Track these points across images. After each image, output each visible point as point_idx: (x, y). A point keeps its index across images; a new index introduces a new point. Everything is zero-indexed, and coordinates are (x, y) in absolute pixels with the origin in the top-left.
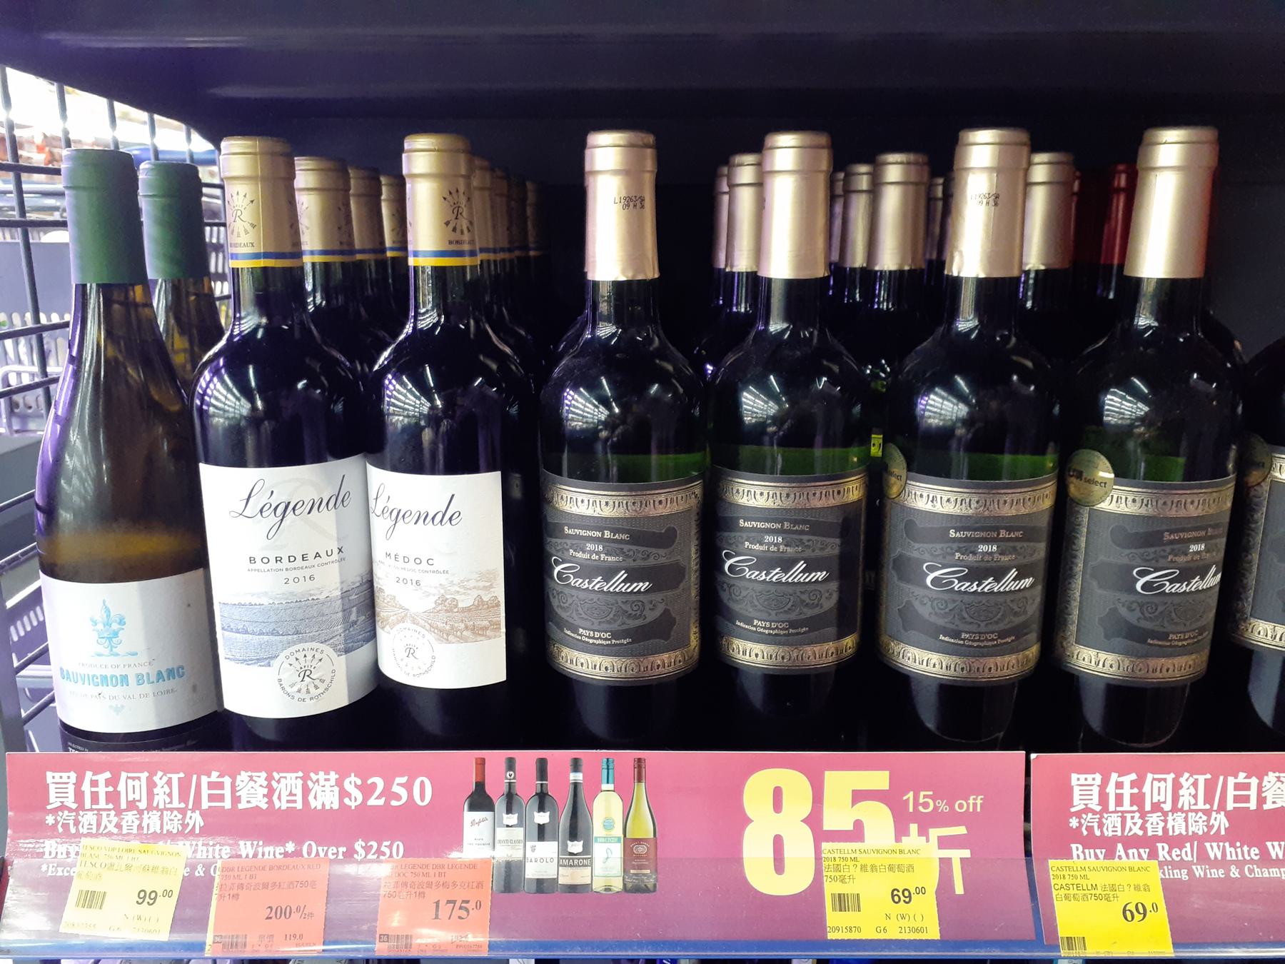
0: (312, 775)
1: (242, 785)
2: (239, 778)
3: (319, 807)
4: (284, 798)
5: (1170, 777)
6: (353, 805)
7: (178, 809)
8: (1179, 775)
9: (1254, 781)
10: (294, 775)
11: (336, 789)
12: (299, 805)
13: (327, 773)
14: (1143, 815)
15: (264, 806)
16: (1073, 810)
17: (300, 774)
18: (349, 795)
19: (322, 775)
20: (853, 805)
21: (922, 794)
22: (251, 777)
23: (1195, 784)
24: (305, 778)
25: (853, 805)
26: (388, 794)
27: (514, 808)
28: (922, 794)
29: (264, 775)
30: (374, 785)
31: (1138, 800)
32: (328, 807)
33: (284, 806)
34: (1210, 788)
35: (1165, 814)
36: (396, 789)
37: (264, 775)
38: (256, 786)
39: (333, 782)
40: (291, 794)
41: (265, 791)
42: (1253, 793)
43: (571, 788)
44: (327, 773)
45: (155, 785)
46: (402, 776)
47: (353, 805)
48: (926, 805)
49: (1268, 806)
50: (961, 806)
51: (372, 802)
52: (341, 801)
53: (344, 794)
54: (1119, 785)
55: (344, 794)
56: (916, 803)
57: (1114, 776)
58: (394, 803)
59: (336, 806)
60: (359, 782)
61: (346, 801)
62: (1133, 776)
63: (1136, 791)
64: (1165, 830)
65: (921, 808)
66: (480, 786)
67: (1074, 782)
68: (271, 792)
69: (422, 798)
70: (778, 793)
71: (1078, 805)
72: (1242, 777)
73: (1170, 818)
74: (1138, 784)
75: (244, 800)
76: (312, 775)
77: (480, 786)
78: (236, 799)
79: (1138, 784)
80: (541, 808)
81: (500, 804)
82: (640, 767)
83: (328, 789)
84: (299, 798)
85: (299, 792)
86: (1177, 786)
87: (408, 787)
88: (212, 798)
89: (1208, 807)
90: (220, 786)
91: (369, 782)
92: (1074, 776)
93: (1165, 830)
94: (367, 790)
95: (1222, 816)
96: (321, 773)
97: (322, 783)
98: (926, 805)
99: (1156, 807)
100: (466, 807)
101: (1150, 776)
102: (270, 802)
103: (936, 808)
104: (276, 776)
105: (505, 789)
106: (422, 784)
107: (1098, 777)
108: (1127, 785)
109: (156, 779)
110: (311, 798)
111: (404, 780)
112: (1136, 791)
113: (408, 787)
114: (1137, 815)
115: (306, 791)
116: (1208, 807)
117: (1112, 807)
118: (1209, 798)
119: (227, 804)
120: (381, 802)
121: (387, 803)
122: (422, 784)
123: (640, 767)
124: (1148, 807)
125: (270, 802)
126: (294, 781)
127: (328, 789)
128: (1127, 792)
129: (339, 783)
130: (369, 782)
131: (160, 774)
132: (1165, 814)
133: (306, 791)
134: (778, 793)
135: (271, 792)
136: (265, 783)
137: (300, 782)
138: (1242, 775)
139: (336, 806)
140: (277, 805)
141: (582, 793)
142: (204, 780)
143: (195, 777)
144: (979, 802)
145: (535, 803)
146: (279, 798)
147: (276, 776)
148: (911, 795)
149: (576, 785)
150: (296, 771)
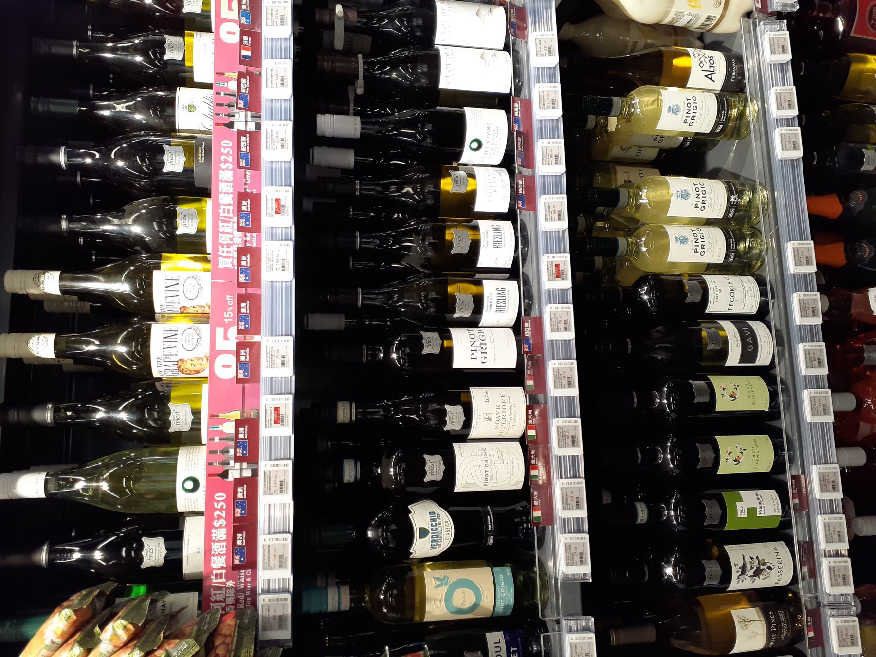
0: (213, 539)
1: (216, 566)
2: (214, 567)
3: (226, 536)
4: (222, 549)
5: (220, 234)
6: (225, 523)
7: (226, 591)
8: (219, 232)
9: (222, 207)
10: (213, 546)
11: (219, 529)
12: (225, 544)
13: (212, 533)
14: (233, 244)
15: (225, 557)
16: (232, 268)
17: (212, 544)
18: (221, 525)
19: (213, 535)
20: (229, 340)
21: (225, 316)
22: (214, 562)
23: (223, 226)
24: (214, 541)
25: (229, 340)
26: (221, 509)
27: (227, 462)
28: (225, 316)
29: (212, 558)
30: (218, 515)
31: (228, 246)
32: (226, 533)
33: (225, 549)
34: (224, 222)
35: (234, 237)
36: (219, 507)
37: (212, 558)
38: (217, 560)
39: (216, 531)
40: (220, 547)
41: (219, 557)
42: (227, 208)
43: (221, 441)
44: (212, 533)
45: (216, 600)
46: (214, 505)
47: (225, 523)
48: (230, 315)
49: (232, 203)
50: (230, 303)
51: (224, 516)
52: (223, 527)
53: (221, 526)
54: (223, 252)
55: (221, 526)
56: (229, 318)
57: (220, 253)
58: (225, 507)
59: (225, 529)
60: (216, 521)
61: (223, 525)
62: (220, 247)
63: (225, 246)
64: (240, 237)
65: (231, 316)
66: (219, 475)
67: (222, 267)
68: (219, 555)
69: (223, 496)
70: (224, 366)
71: (230, 266)
72: (221, 211)
73: (235, 235)
74: (223, 245)
75: (222, 565)
76: (213, 539)
77: (219, 475)
78: (222, 568)
79: (223, 245)
80: (228, 452)
81: (226, 468)
82: (213, 416)
83: (218, 533)
84: (222, 544)
85: (219, 544)
86: (223, 233)
87: (218, 502)
88: (221, 577)
89: (231, 223)
90: (216, 575)
91: (216, 517)
92: (219, 266)
93: (240, 237)
94: (219, 517)
95: (234, 218)
96: (212, 535)
97: (216, 535)
98: (230, 315)
99: (231, 240)
100: (227, 480)
101: (220, 241)
102: (224, 555)
103: (231, 311)
104: (212, 553)
105: (221, 466)
106: (218, 497)
107: (220, 259)
108: (223, 249)
109: (213, 600)
110: (222, 539)
111: (216, 504)
112: (225, 246)
113: (218, 502)
114: (234, 246)
115: (219, 541)
116: (231, 223)
117: (231, 255)
118: (228, 222)
119: (224, 571)
120: (224, 512)
121: (224, 510)
122: (218, 497)
123: (213, 416)
124: (231, 242)
125: (224, 555)
126: (215, 546)
127: (218, 533)
128: (225, 249)
129: (216, 528)
130: (216, 517)
131: (211, 598)
132: (234, 237)
133: (219, 541)
134: (224, 366)
135: (219, 555)
136: (216, 557)
137: (216, 544)
138: (220, 211)
139: (225, 529)
140: (225, 552)
141: (222, 437)
142: (214, 581)
143: (213, 585)
144: (229, 296)
145: (226, 455)
146: (222, 551)
147: (213, 553)
148: (226, 320)
149: (220, 439)
150: (211, 545)
